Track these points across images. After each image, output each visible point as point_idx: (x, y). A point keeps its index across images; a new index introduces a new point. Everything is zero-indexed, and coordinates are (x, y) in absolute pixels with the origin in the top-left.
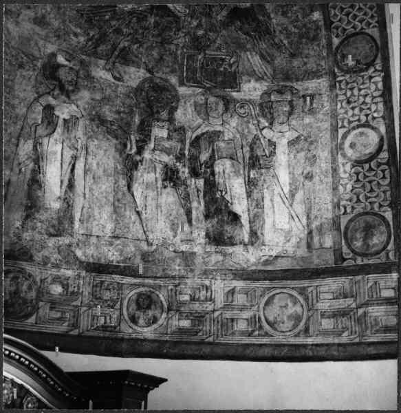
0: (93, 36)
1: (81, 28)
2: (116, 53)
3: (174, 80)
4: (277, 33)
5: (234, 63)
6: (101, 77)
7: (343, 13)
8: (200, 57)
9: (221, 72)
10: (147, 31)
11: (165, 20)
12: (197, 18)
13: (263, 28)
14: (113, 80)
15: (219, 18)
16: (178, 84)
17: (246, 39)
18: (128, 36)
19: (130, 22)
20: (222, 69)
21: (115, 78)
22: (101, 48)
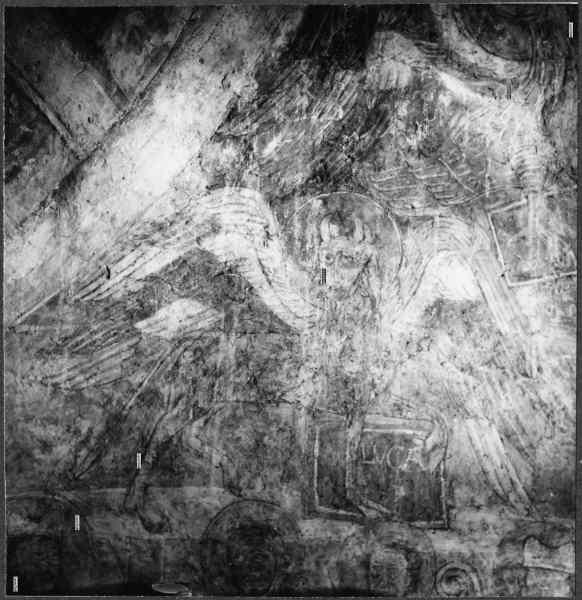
0: (90, 430)
1: (56, 422)
3: (289, 499)
4: (547, 374)
5: (435, 447)
9: (402, 473)
12: (341, 332)
14: (146, 536)
16: (299, 513)
17: (466, 384)
18: (176, 404)
19: (177, 365)
21: (149, 527)
22: (110, 457)
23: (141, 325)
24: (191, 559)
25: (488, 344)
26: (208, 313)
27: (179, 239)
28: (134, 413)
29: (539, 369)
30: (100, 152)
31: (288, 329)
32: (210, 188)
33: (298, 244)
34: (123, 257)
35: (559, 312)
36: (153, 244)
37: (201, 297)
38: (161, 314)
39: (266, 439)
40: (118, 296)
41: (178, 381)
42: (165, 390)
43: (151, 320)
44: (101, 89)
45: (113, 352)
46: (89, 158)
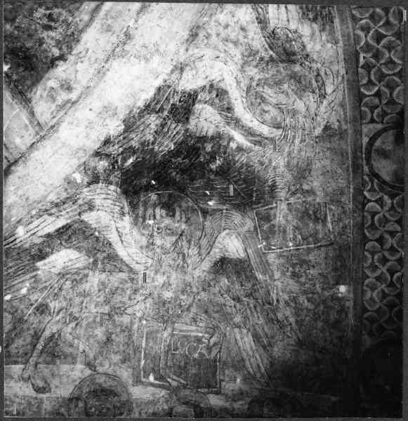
2: (39, 347)
3: (125, 374)
4: (282, 304)
5: (215, 344)
6: (16, 396)
7: (385, 301)
8: (166, 334)
10: (88, 298)
11: (116, 279)
13: (262, 292)
15: (197, 273)
18: (58, 313)
20: (196, 356)
23: (39, 264)
24: (63, 410)
25: (250, 285)
26: (82, 259)
27: (68, 212)
28: (31, 318)
29: (278, 301)
30: (23, 159)
31: (131, 270)
32: (89, 184)
33: (141, 220)
34: (32, 222)
35: (291, 269)
36: (51, 215)
37: (78, 249)
38: (52, 258)
39: (113, 336)
40: (27, 246)
41: (61, 299)
42: (52, 305)
43: (47, 261)
44: (27, 122)
45: (21, 280)
46: (16, 162)
